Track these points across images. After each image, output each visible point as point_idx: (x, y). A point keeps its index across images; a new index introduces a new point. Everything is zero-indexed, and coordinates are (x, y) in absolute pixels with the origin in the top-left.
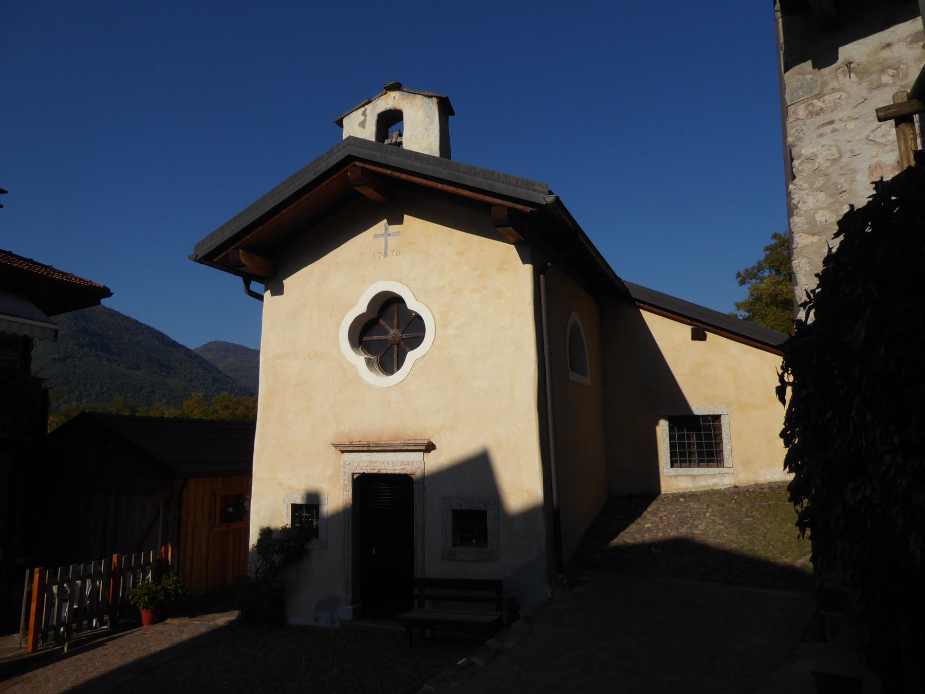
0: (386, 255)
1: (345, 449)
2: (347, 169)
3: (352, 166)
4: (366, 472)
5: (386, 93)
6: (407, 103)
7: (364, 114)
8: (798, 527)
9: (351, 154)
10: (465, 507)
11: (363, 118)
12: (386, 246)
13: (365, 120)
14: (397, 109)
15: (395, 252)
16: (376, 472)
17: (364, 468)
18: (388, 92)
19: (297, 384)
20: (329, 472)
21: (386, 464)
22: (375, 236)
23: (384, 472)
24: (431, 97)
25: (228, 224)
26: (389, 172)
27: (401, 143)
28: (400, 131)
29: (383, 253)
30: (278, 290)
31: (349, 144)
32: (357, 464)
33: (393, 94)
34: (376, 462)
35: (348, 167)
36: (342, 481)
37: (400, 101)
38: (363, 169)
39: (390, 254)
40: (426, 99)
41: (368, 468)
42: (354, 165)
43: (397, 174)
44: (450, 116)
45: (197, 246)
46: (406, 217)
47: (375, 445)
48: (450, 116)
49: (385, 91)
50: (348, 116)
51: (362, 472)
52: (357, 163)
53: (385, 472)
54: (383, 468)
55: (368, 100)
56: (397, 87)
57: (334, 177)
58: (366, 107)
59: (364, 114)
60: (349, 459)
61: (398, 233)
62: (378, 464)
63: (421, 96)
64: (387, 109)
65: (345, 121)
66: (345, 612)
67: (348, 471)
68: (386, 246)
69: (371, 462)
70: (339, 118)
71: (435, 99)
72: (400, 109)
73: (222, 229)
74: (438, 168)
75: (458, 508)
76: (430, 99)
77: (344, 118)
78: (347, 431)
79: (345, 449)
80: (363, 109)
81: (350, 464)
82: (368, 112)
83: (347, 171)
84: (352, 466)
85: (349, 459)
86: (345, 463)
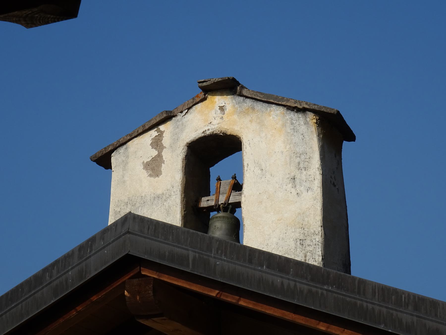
2: (124, 283)
3: (132, 278)
5: (204, 99)
6: (251, 121)
9: (132, 253)
11: (155, 153)
13: (159, 156)
14: (228, 133)
18: (209, 97)
24: (303, 110)
26: (214, 293)
27: (238, 205)
28: (234, 178)
31: (128, 232)
35: (126, 278)
37: (235, 117)
38: (158, 283)
42: (139, 275)
43: (230, 298)
44: (345, 142)
48: (345, 142)
49: (202, 96)
50: (122, 150)
52: (145, 272)
55: (165, 115)
57: (94, 298)
58: (162, 127)
64: (208, 133)
65: (115, 159)
71: (311, 117)
72: (234, 133)
74: (320, 291)
76: (300, 115)
77: (112, 151)
80: (153, 133)
82: (166, 141)
83: (123, 287)
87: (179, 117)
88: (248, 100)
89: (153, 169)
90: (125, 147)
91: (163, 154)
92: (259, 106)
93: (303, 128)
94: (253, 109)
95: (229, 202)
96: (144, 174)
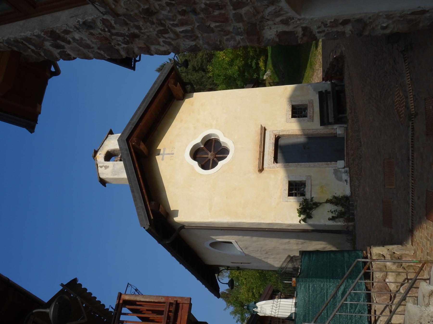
0: (173, 154)
1: (261, 170)
4: (273, 156)
5: (96, 158)
7: (101, 167)
8: (338, 161)
10: (290, 113)
12: (169, 154)
15: (173, 150)
16: (273, 152)
17: (271, 157)
19: (227, 198)
20: (273, 176)
21: (270, 147)
22: (163, 159)
23: (274, 148)
24: (107, 137)
25: (136, 205)
29: (172, 155)
30: (176, 213)
32: (270, 161)
33: (98, 155)
34: (269, 152)
36: (277, 169)
39: (173, 152)
40: (107, 139)
41: (271, 155)
45: (142, 225)
46: (158, 148)
47: (260, 148)
50: (100, 174)
51: (273, 159)
53: (274, 148)
54: (272, 148)
56: (96, 152)
59: (101, 167)
60: (267, 165)
61: (164, 149)
62: (270, 151)
63: (105, 141)
64: (104, 157)
66: (341, 164)
67: (272, 165)
68: (169, 154)
69: (269, 154)
70: (98, 180)
71: (109, 135)
72: (106, 152)
73: (137, 208)
75: (291, 116)
76: (108, 137)
78: (253, 168)
79: (261, 170)
81: (269, 165)
82: (101, 165)
84: (270, 163)
85: (267, 165)
86: (269, 167)
87: (98, 163)
88: (100, 148)
89: (107, 168)
90: (99, 174)
91: (104, 165)
92: (103, 146)
93: (111, 137)
94: (103, 147)
95: (114, 309)
96: (107, 169)
